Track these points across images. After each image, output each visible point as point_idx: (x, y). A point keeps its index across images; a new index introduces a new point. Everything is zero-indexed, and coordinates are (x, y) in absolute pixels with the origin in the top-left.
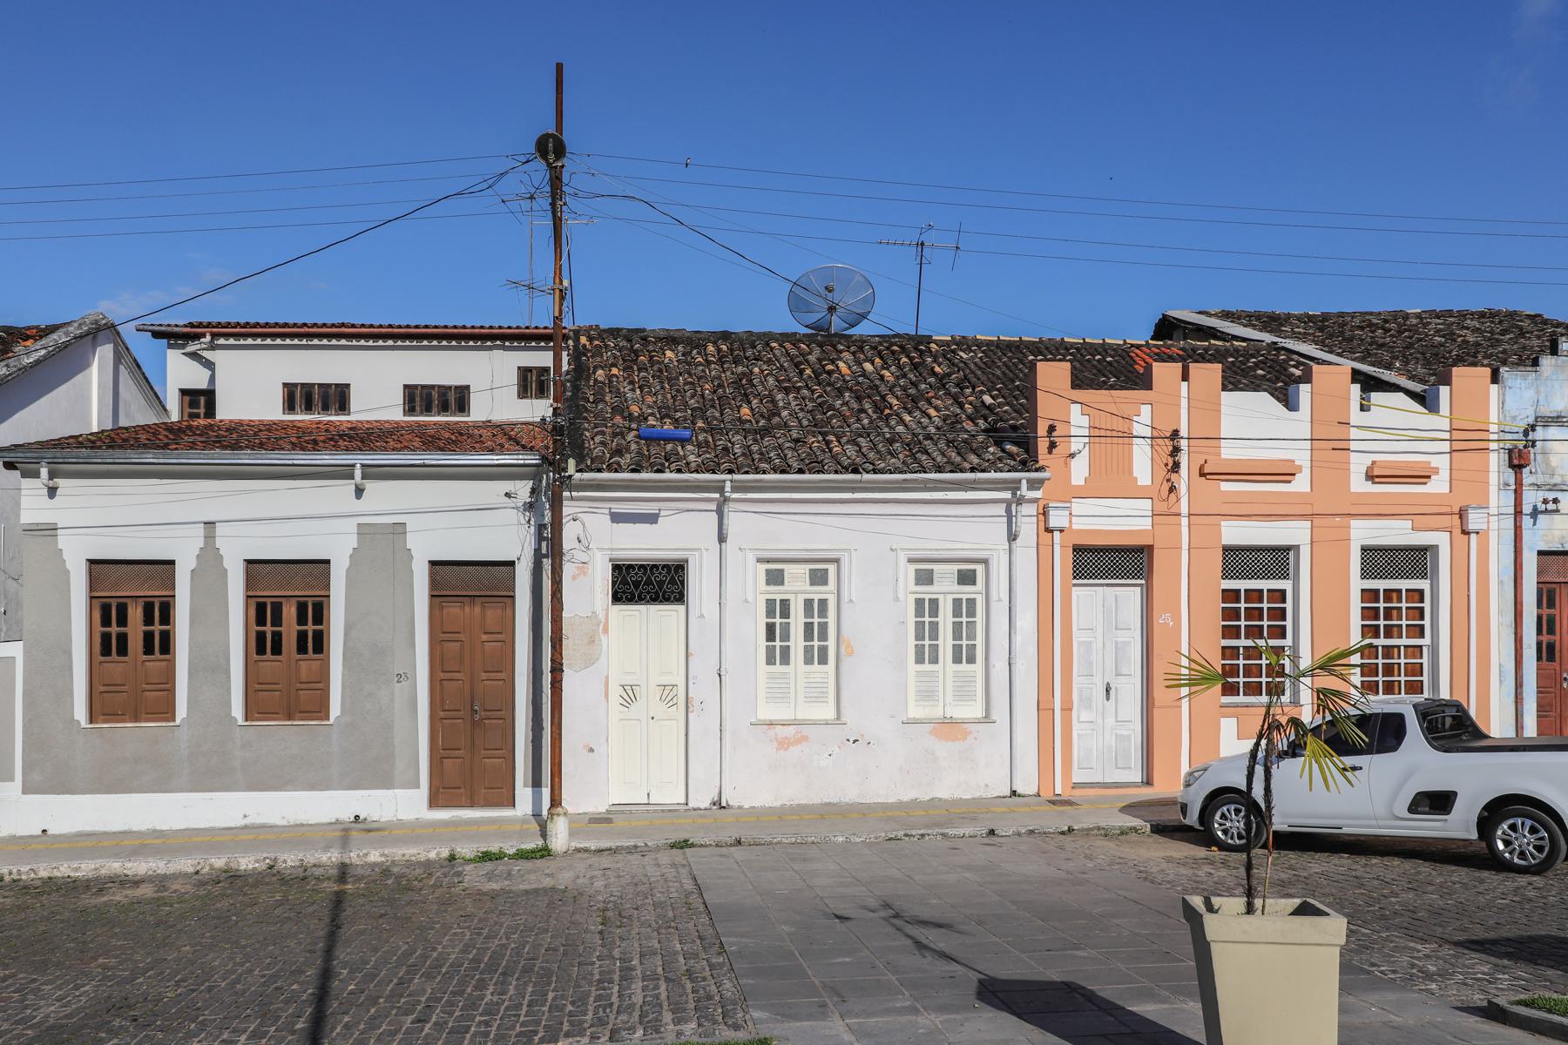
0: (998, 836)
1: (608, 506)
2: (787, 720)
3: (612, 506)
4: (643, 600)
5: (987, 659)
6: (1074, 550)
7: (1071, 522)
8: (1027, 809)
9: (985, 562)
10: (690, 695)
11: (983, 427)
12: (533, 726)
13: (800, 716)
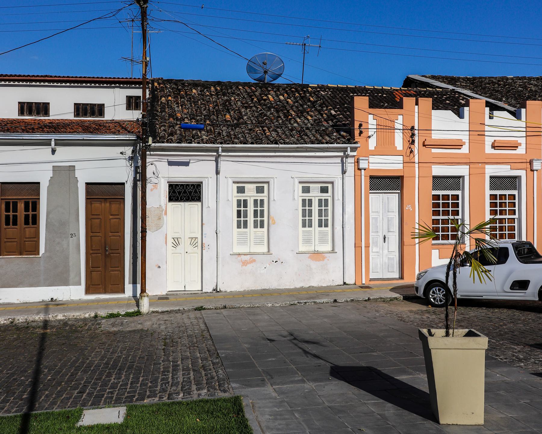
0: (338, 302)
2: (246, 253)
4: (182, 200)
5: (333, 225)
6: (370, 178)
7: (369, 165)
8: (351, 290)
9: (332, 183)
10: (203, 242)
11: (331, 124)
13: (252, 251)
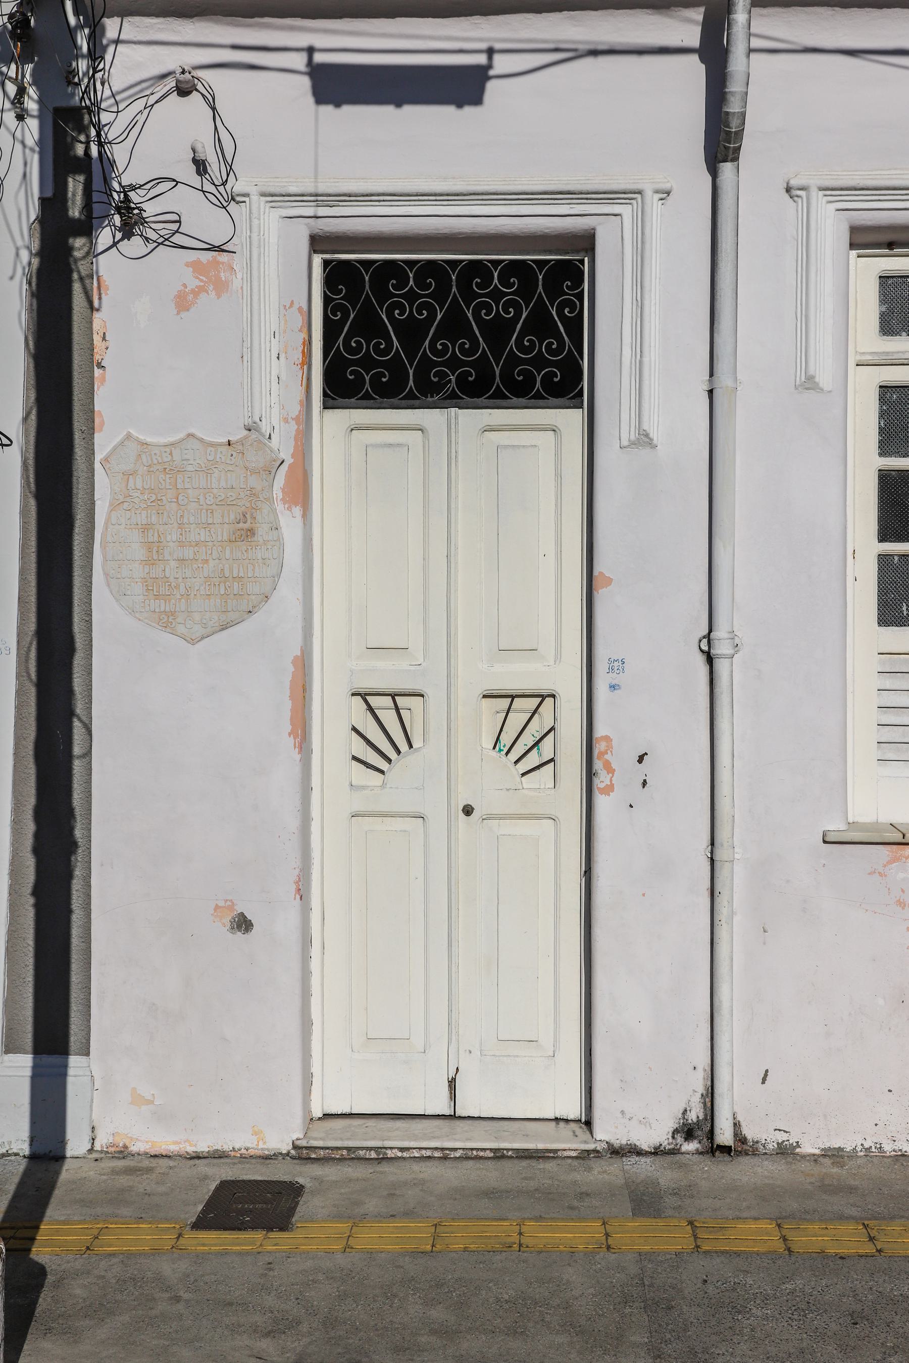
1: (303, 40)
3: (319, 41)
10: (600, 731)
12: (37, 836)
